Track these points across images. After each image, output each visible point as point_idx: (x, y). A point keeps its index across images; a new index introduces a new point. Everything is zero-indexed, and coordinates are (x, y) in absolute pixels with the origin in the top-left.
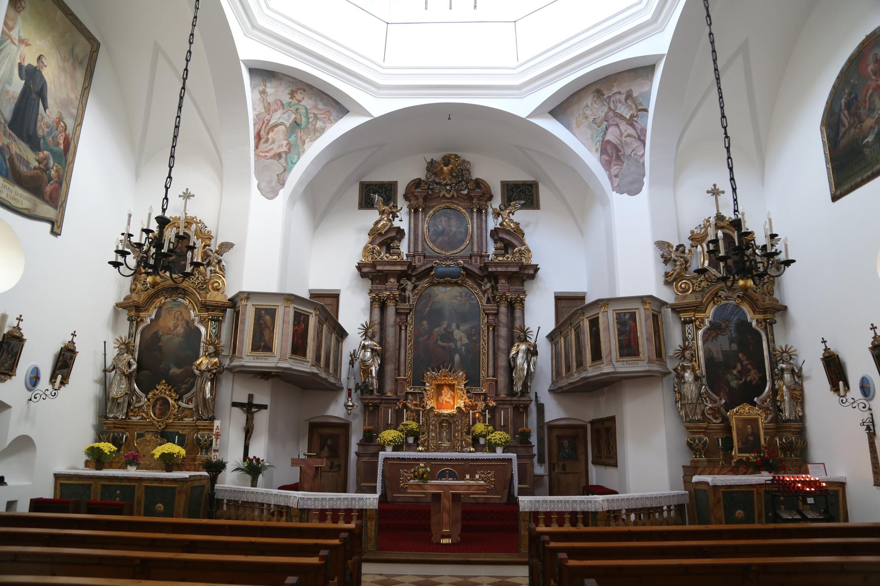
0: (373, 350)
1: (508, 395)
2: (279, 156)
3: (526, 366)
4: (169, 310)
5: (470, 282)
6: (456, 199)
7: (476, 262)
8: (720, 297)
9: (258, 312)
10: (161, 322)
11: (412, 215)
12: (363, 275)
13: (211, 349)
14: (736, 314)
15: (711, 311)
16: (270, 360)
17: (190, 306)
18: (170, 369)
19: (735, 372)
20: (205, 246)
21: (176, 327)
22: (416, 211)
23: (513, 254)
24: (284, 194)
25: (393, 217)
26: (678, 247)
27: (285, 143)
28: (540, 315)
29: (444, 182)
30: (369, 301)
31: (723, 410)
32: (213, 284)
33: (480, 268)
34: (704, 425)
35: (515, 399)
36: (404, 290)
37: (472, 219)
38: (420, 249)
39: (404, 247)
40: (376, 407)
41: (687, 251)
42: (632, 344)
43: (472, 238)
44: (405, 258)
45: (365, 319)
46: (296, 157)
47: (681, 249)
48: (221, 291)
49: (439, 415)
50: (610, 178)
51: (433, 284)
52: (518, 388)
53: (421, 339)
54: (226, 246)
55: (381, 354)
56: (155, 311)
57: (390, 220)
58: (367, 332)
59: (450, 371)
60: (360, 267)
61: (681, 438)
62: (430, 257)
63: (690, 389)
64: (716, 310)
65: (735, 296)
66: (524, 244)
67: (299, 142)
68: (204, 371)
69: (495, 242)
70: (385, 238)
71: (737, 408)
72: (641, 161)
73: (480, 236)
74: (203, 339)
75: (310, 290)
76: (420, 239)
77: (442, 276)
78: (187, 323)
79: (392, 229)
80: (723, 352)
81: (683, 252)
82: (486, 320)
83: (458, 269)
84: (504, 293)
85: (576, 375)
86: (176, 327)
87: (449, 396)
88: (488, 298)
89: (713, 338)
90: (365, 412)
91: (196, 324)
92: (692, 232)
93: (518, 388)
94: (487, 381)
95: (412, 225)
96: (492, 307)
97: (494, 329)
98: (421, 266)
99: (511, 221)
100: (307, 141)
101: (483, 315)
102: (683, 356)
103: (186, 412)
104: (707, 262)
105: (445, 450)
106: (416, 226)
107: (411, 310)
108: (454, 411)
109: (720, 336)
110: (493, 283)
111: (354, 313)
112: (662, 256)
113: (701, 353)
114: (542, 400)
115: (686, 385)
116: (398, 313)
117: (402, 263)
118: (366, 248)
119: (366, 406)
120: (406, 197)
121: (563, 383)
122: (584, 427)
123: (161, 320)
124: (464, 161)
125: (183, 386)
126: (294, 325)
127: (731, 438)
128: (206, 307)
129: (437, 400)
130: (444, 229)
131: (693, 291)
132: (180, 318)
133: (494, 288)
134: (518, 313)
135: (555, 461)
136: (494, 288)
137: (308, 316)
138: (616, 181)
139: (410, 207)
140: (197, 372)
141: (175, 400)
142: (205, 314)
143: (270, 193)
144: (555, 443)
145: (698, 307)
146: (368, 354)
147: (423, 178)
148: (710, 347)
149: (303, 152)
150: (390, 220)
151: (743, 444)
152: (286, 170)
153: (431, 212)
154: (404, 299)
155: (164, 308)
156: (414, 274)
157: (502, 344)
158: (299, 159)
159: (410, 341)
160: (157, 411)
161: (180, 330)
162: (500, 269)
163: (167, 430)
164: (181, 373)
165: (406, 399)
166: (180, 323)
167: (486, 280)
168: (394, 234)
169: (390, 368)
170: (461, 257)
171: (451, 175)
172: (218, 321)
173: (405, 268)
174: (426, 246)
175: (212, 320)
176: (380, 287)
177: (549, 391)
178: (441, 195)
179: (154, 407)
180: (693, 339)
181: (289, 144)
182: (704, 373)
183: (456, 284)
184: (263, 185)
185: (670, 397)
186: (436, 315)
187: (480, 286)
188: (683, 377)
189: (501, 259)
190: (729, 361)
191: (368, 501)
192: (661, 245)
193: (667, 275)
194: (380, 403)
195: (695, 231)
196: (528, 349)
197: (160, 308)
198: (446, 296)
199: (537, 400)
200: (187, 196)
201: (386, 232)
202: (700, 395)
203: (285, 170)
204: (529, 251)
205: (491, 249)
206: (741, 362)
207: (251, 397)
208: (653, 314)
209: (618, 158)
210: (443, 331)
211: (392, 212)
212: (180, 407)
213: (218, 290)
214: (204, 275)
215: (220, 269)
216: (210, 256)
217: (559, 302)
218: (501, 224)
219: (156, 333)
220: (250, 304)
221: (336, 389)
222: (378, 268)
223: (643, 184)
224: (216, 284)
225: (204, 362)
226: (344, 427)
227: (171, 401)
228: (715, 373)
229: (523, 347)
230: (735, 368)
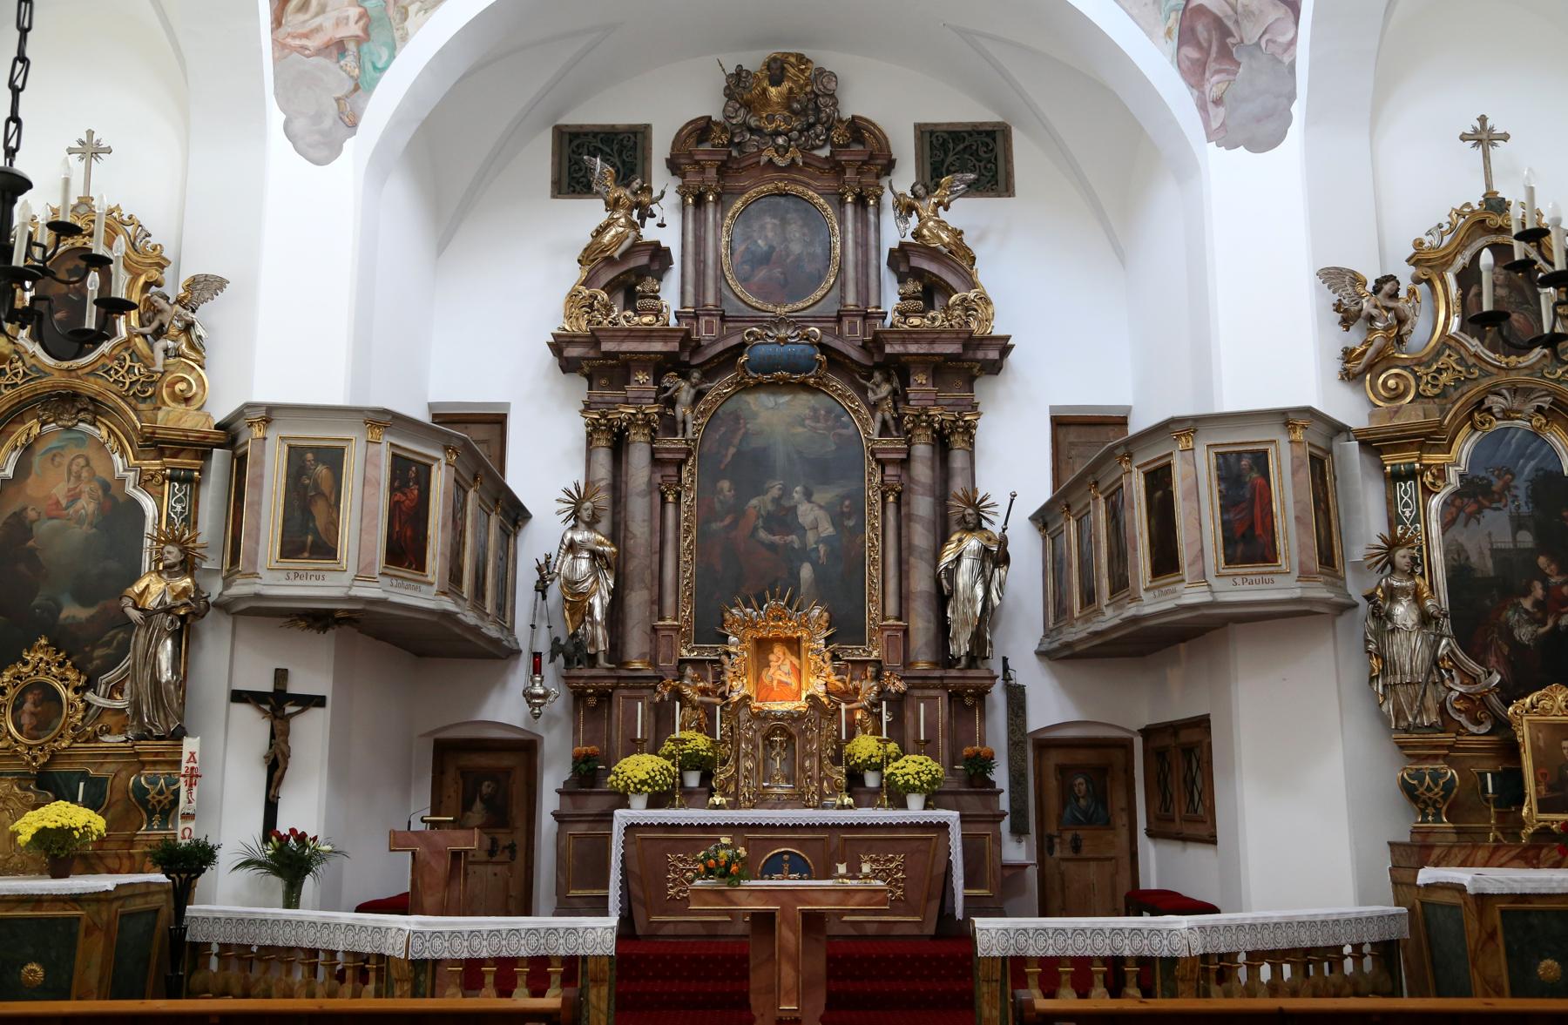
0: (595, 555)
1: (935, 664)
2: (340, 47)
3: (979, 591)
4: (54, 454)
5: (837, 383)
6: (800, 170)
7: (853, 330)
8: (1489, 410)
9: (296, 455)
10: (32, 487)
11: (690, 210)
12: (568, 366)
13: (173, 554)
14: (1532, 456)
15: (1464, 447)
16: (331, 578)
17: (112, 443)
18: (60, 610)
19: (1527, 604)
20: (147, 285)
21: (74, 498)
22: (700, 201)
23: (947, 309)
24: (357, 150)
25: (642, 217)
26: (1380, 283)
27: (354, 12)
28: (1013, 465)
29: (770, 127)
30: (582, 431)
31: (1494, 700)
32: (172, 385)
33: (864, 346)
34: (1448, 738)
35: (953, 673)
36: (671, 402)
37: (842, 222)
38: (710, 300)
39: (670, 293)
40: (605, 697)
41: (1402, 294)
42: (1258, 531)
43: (841, 270)
44: (673, 322)
45: (574, 475)
46: (385, 54)
47: (1387, 287)
48: (195, 404)
50: (1202, 107)
51: (743, 388)
52: (961, 645)
53: (715, 526)
54: (205, 287)
55: (614, 564)
56: (14, 456)
57: (633, 225)
58: (578, 509)
59: (789, 604)
60: (558, 345)
61: (1387, 770)
62: (736, 319)
63: (1409, 649)
64: (1478, 447)
65: (1530, 408)
66: (973, 285)
67: (392, 12)
68: (155, 611)
69: (901, 280)
70: (624, 272)
71: (1534, 696)
72: (1286, 59)
73: (863, 265)
74: (149, 528)
75: (431, 406)
76: (710, 272)
77: (768, 366)
78: (106, 487)
79: (637, 246)
80: (1495, 552)
81: (1394, 296)
82: (878, 479)
83: (809, 350)
84: (925, 409)
85: (1109, 612)
86: (74, 498)
87: (787, 668)
88: (884, 423)
89: (1470, 516)
90: (576, 709)
91: (130, 489)
92: (1418, 244)
93: (961, 645)
94: (883, 629)
95: (690, 238)
96: (892, 446)
98: (713, 343)
99: (942, 224)
100: (412, 9)
101: (870, 465)
102: (1392, 562)
103: (108, 720)
104: (1455, 322)
105: (781, 803)
106: (700, 241)
107: (689, 453)
108: (801, 705)
109: (1487, 512)
110: (896, 383)
111: (547, 459)
112: (1338, 307)
113: (1437, 556)
114: (1019, 678)
115: (1398, 637)
116: (656, 462)
117: (665, 334)
118: (573, 296)
119: (579, 696)
120: (673, 166)
121: (1076, 632)
122: (1125, 745)
123: (30, 480)
124: (821, 72)
125: (98, 652)
126: (392, 489)
127: (1518, 774)
128: (155, 444)
129: (758, 678)
130: (772, 248)
131: (1418, 395)
132: (84, 474)
133: (899, 397)
134: (958, 460)
135: (1052, 829)
136: (899, 397)
137: (429, 467)
138: (1218, 115)
139: (683, 192)
140: (135, 615)
141: (76, 690)
142: (153, 465)
143: (320, 145)
144: (1052, 783)
145: (1431, 438)
146: (583, 565)
147: (717, 116)
148: (1462, 539)
149: (404, 39)
150: (633, 225)
151: (1550, 788)
152: (361, 87)
153: (739, 204)
154: (671, 426)
155: (40, 448)
156: (695, 362)
157: (921, 537)
158: (392, 57)
159: (688, 531)
160: (26, 720)
161: (87, 506)
162: (913, 348)
163: (56, 768)
164: (91, 620)
165: (681, 678)
166: (86, 488)
167: (877, 376)
168: (643, 260)
169: (637, 600)
170: (816, 320)
171: (789, 107)
172: (190, 482)
173: (674, 346)
174: (726, 292)
175: (171, 479)
176: (609, 395)
177: (1039, 654)
178: (764, 159)
179: (17, 709)
180: (1416, 520)
181: (364, 15)
182: (1445, 605)
183: (804, 387)
184: (300, 124)
185: (1355, 668)
186: (753, 466)
187: (862, 391)
188: (1390, 616)
189: (916, 321)
190: (1511, 576)
191: (590, 937)
192: (1333, 277)
193: (1348, 354)
194: (614, 688)
195: (1427, 240)
196: (985, 552)
197: (28, 449)
198: (777, 416)
199: (1007, 677)
200: (90, 150)
201: (626, 255)
202: (1435, 662)
203: (357, 88)
204: (988, 302)
205: (890, 297)
206: (1544, 578)
207: (281, 675)
208: (1312, 457)
209: (1226, 53)
210: (770, 507)
211: (638, 205)
212: (88, 706)
213: (187, 400)
214: (148, 362)
215: (192, 346)
216: (160, 311)
217: (1062, 431)
218: (917, 234)
219: (19, 516)
220: (273, 435)
221: (504, 653)
222: (607, 346)
223: (1288, 120)
224: (181, 386)
225: (153, 588)
226: (526, 749)
227: (66, 694)
228: (1474, 608)
229: (972, 543)
230: (1527, 592)
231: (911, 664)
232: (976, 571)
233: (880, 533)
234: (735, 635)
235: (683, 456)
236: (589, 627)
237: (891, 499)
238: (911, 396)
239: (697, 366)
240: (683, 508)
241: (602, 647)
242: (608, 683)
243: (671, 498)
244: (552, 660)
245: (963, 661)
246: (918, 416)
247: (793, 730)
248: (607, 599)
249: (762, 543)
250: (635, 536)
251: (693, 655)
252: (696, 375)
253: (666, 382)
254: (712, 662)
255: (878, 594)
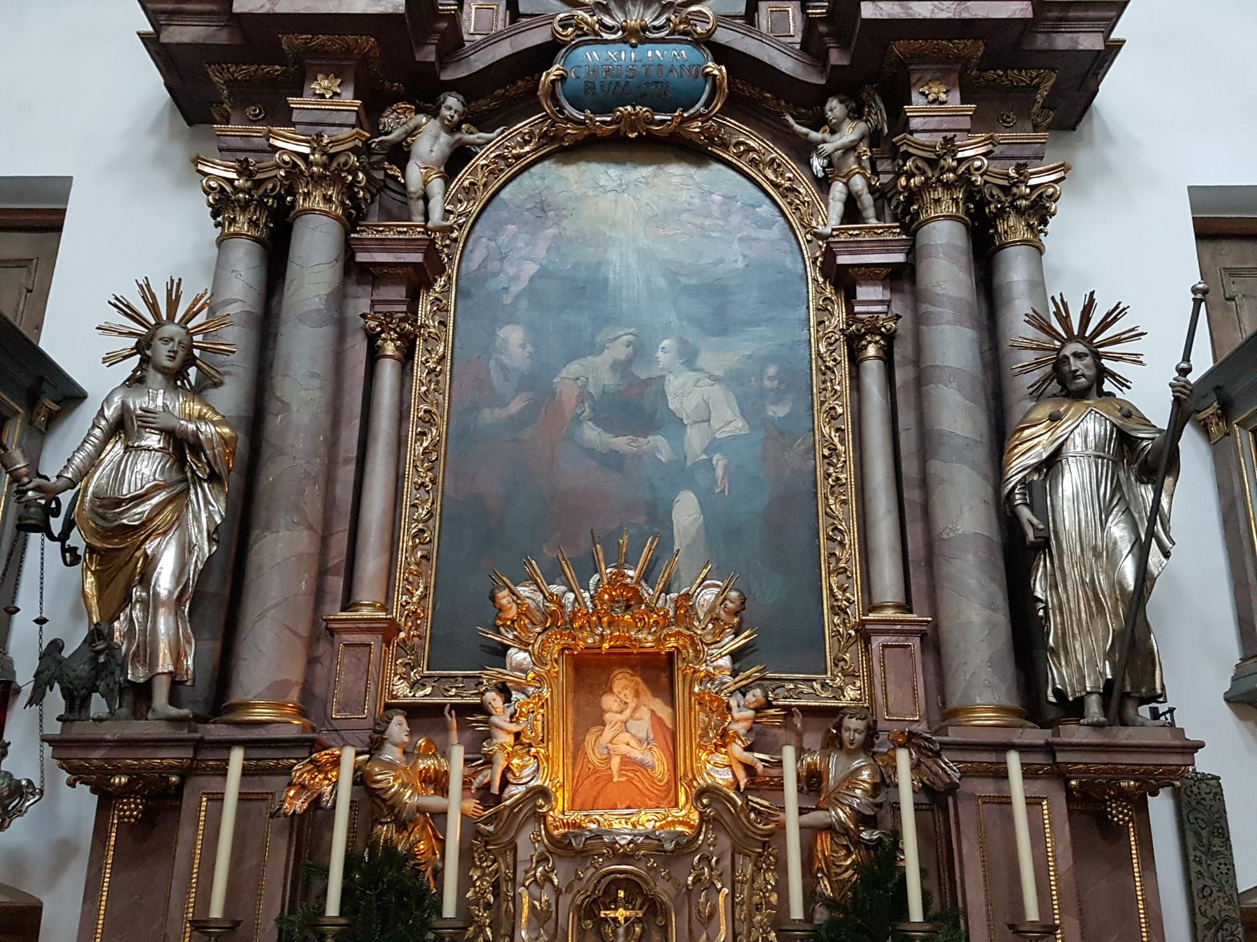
0: (181, 446)
36: (400, 154)
49: (567, 847)
52: (1081, 664)
53: (489, 416)
59: (647, 576)
77: (604, 94)
87: (642, 726)
97: (887, 357)
116: (354, 272)
129: (577, 750)
134: (1015, 269)
136: (885, 143)
157: (957, 414)
159: (428, 420)
167: (835, 108)
169: (282, 552)
177: (1227, 700)
187: (802, 151)
210: (609, 380)
229: (1086, 429)
231: (955, 713)
232: (1106, 489)
233: (848, 426)
234: (524, 645)
235: (417, 258)
236: (137, 613)
237: (871, 350)
238: (915, 123)
239: (454, 86)
240: (419, 372)
241: (165, 664)
242: (169, 757)
243: (390, 348)
244: (37, 698)
245: (1094, 708)
246: (933, 163)
247: (663, 890)
248: (205, 549)
249: (591, 452)
250: (286, 407)
251: (423, 695)
252: (452, 103)
253: (388, 119)
254: (462, 710)
255: (850, 555)
